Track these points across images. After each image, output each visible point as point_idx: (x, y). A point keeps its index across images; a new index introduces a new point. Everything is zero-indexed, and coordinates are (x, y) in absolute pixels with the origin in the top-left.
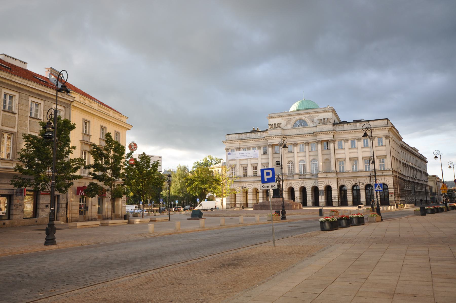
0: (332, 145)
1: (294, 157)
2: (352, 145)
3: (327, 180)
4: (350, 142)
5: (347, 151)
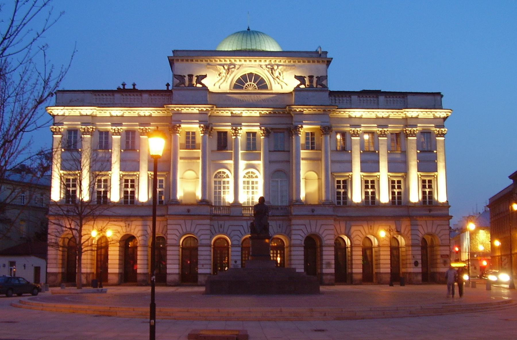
3: (313, 222)
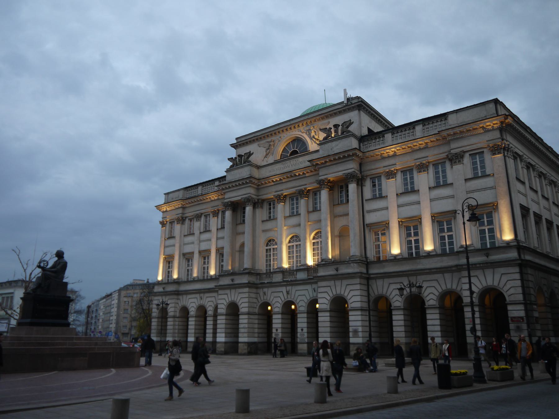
2: (406, 184)
3: (338, 283)
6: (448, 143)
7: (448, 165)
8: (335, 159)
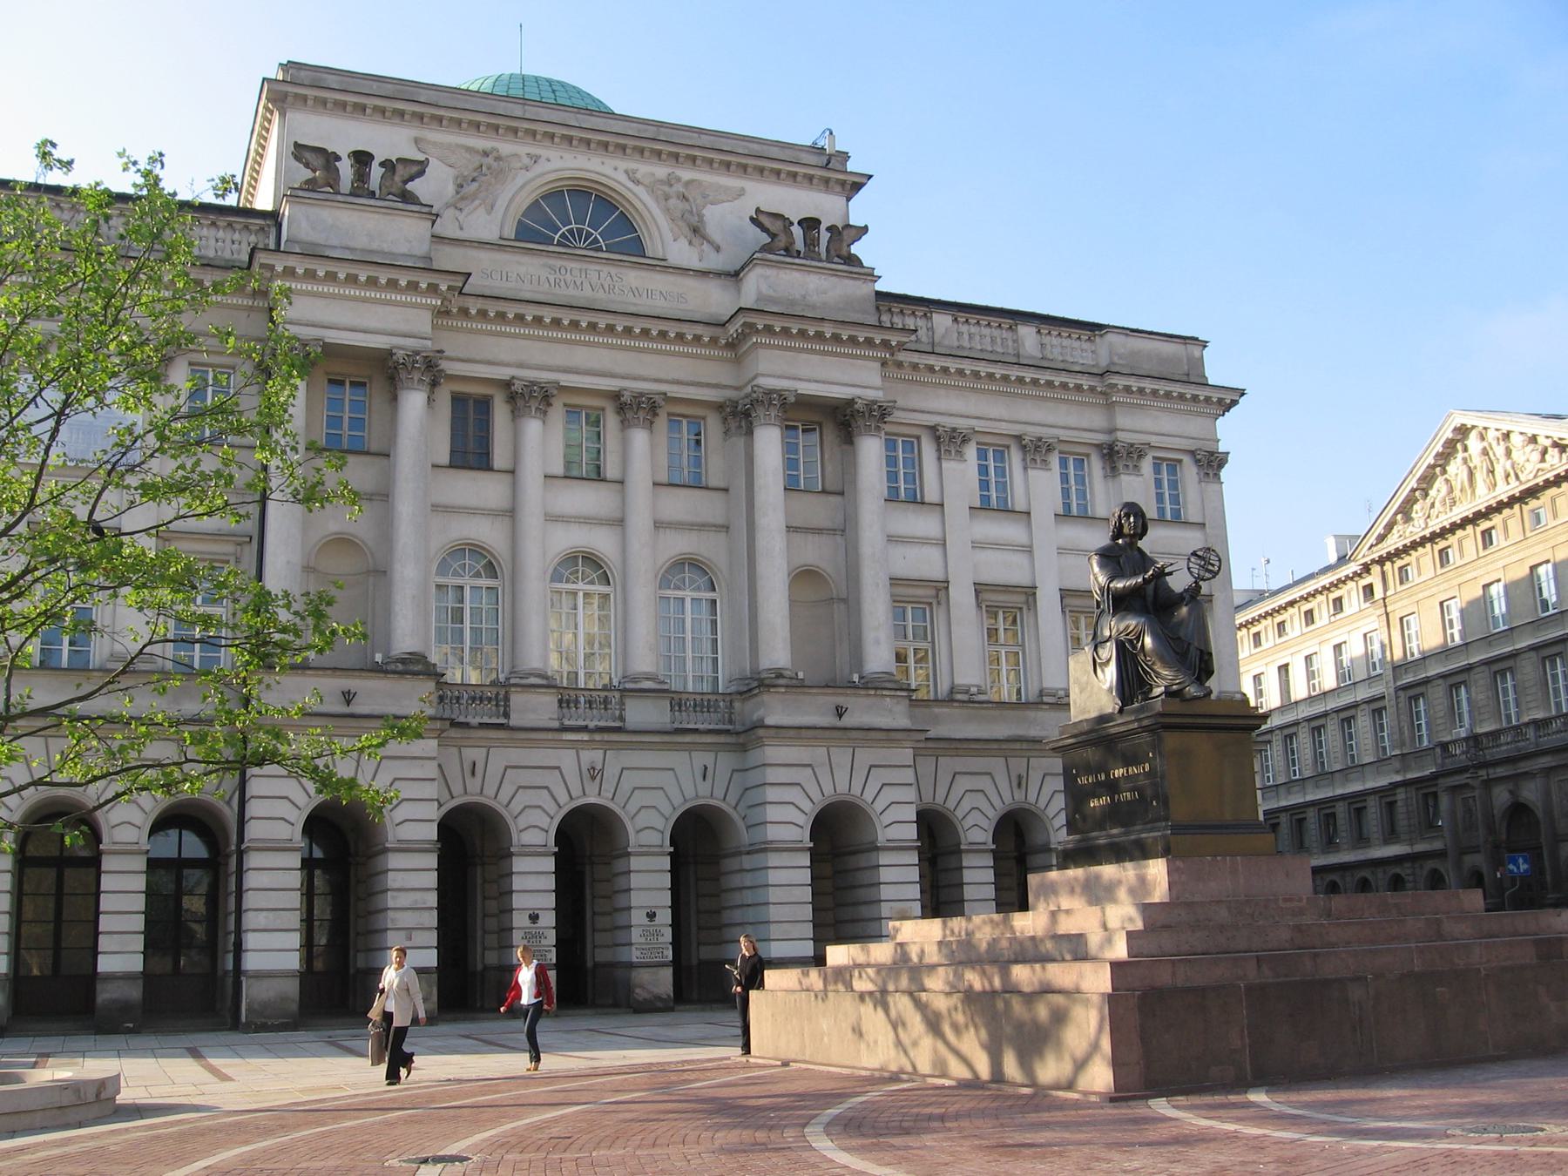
0: (871, 450)
1: (511, 513)
2: (984, 485)
3: (841, 756)
4: (971, 452)
5: (964, 528)
6: (1110, 406)
7: (1096, 466)
8: (836, 338)
